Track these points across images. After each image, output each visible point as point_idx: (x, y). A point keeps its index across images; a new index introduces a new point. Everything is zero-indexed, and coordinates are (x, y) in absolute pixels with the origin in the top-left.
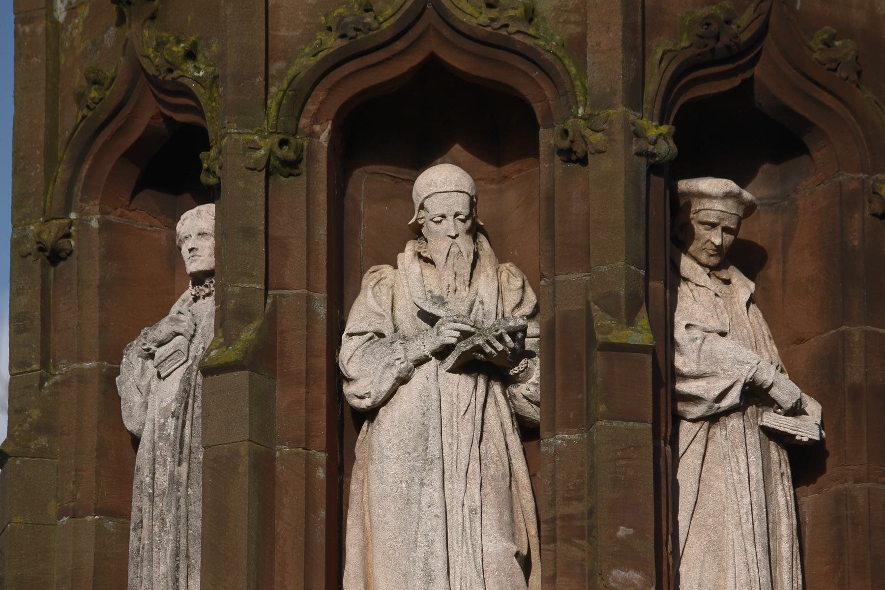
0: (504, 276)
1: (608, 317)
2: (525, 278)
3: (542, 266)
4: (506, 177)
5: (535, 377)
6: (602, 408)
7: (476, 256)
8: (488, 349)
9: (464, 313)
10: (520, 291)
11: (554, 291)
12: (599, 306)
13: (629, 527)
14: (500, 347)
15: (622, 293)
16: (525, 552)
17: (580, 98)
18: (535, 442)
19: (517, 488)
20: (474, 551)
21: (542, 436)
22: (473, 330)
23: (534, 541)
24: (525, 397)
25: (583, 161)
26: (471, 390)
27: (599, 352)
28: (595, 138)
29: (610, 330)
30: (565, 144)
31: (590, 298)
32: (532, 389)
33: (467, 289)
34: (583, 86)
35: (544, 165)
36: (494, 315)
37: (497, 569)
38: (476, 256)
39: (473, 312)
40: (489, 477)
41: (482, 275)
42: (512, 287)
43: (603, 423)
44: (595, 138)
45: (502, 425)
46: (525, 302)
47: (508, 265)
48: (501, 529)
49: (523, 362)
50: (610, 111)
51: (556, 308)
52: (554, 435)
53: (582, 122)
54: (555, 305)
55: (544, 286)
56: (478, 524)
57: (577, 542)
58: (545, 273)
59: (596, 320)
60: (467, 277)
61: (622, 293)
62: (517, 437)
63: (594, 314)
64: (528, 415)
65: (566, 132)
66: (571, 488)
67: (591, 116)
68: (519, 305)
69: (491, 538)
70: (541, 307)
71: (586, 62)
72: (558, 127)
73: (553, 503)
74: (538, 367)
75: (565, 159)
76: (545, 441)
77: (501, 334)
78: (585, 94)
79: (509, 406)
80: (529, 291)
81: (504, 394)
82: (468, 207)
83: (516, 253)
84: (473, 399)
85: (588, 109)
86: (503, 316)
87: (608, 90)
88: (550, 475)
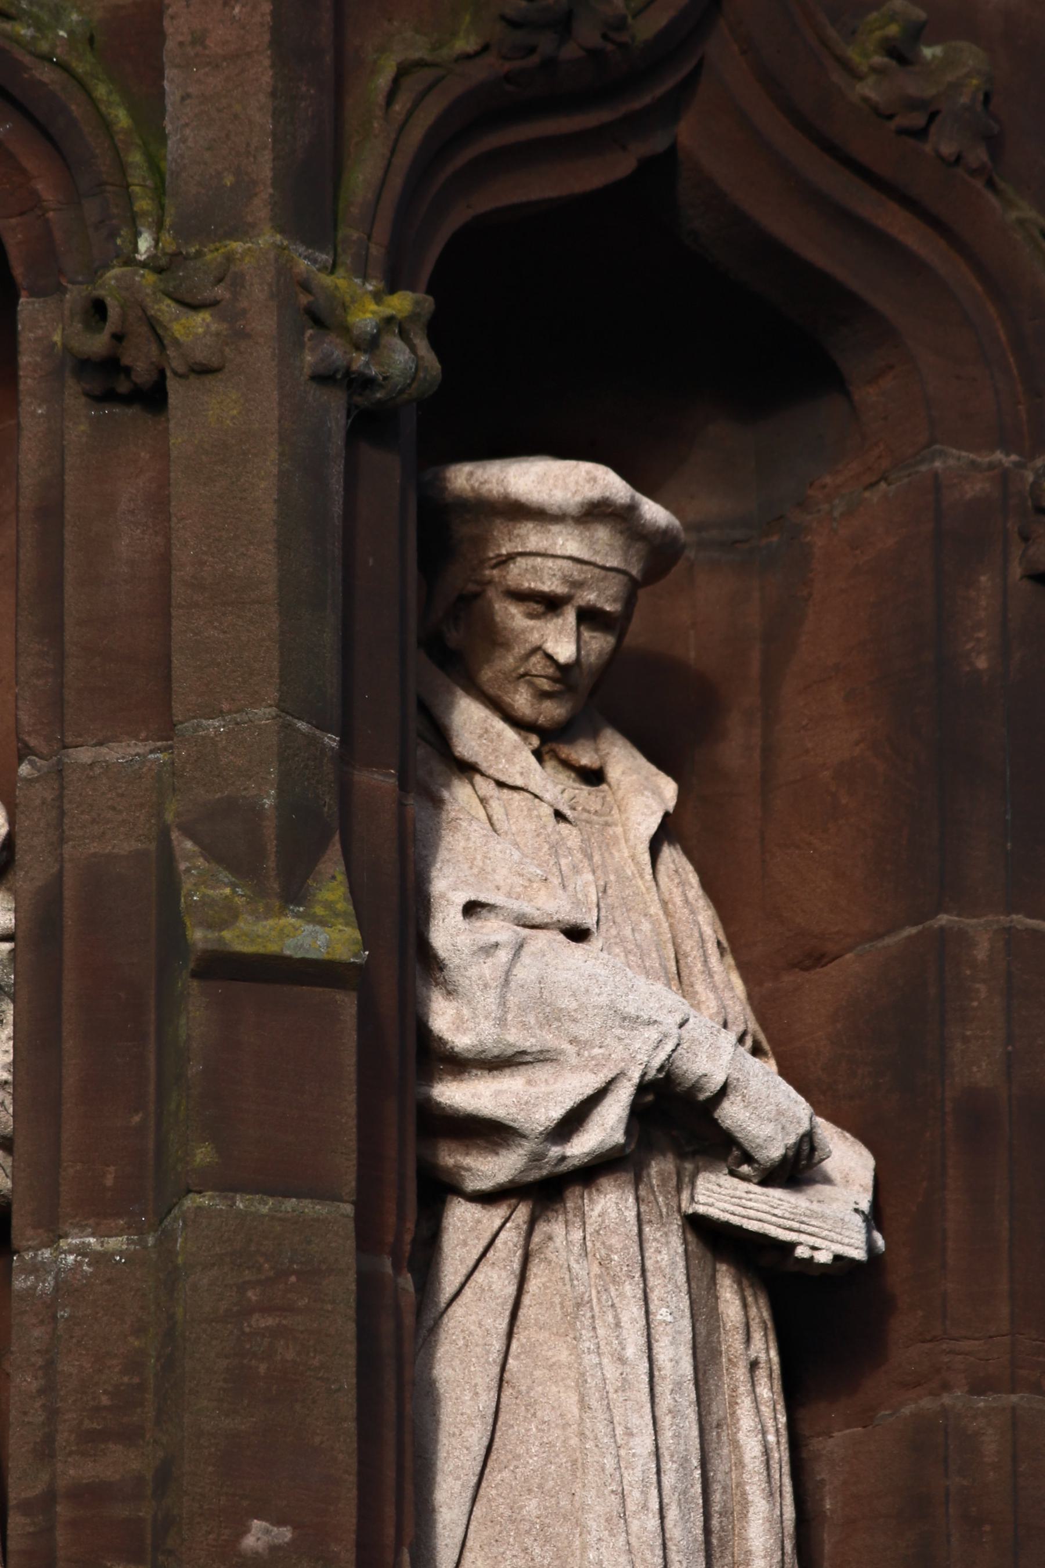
1: (225, 876)
3: (24, 718)
6: (203, 1155)
11: (60, 797)
12: (196, 841)
13: (279, 1523)
15: (268, 802)
17: (144, 204)
21: (17, 1241)
25: (153, 398)
27: (195, 983)
28: (193, 329)
29: (229, 915)
30: (97, 344)
31: (169, 817)
34: (154, 166)
35: (33, 411)
43: (204, 1200)
44: (193, 329)
50: (237, 246)
51: (67, 848)
52: (54, 1238)
53: (148, 279)
54: (62, 840)
55: (29, 781)
58: (33, 742)
59: (187, 885)
61: (268, 802)
63: (183, 866)
65: (98, 309)
66: (105, 1400)
67: (177, 259)
70: (20, 843)
71: (162, 94)
72: (75, 295)
73: (45, 1451)
76: (28, 1256)
78: (159, 192)
85: (166, 237)
87: (229, 180)
88: (40, 1361)
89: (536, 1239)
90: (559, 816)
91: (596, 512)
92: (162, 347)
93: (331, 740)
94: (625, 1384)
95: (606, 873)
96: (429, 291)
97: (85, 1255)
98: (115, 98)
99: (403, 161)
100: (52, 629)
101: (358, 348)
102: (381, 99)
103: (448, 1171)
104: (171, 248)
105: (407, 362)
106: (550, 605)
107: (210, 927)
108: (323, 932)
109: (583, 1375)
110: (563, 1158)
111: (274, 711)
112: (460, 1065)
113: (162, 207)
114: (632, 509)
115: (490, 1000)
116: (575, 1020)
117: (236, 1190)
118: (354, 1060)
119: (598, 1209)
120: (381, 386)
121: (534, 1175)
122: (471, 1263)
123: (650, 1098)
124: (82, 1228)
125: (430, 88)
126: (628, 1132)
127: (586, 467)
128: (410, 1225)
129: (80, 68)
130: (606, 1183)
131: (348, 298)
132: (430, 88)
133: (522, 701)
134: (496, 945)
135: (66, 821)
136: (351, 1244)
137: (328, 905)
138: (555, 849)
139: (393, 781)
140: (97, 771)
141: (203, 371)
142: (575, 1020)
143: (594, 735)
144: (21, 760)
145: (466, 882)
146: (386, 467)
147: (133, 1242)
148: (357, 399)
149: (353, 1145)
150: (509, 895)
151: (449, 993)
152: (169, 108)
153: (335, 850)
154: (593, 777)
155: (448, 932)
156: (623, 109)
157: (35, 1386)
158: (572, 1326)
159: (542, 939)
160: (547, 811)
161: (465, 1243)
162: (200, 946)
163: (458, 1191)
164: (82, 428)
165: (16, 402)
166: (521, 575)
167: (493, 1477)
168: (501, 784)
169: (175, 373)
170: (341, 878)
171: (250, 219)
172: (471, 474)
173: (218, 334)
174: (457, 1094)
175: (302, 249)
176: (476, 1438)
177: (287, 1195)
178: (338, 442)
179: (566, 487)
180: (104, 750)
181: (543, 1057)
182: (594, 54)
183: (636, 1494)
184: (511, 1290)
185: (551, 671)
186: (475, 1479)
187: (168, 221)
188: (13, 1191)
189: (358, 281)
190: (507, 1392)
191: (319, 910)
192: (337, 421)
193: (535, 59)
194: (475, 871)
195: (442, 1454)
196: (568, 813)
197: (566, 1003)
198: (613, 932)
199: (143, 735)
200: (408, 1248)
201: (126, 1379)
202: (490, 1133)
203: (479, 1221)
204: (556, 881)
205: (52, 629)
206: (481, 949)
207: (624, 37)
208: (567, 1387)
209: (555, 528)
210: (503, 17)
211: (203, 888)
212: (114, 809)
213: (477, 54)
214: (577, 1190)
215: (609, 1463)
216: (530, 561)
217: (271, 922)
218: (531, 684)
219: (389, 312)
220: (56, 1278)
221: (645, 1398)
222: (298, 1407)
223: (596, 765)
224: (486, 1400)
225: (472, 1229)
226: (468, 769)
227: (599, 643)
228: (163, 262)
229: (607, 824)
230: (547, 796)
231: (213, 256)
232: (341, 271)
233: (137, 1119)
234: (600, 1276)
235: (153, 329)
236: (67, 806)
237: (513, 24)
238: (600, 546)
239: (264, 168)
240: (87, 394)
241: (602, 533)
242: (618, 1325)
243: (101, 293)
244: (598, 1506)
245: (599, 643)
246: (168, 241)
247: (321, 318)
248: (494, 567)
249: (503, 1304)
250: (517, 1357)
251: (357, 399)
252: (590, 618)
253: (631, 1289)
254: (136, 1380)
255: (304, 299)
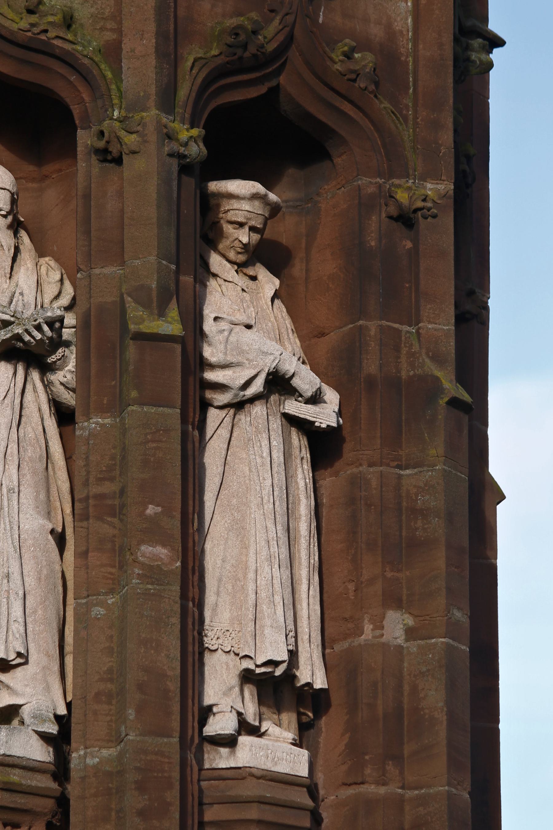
0: (43, 270)
1: (141, 308)
2: (63, 271)
3: (79, 259)
4: (47, 177)
5: (71, 365)
6: (134, 394)
7: (17, 250)
8: (27, 338)
9: (5, 304)
10: (59, 284)
11: (90, 284)
12: (132, 298)
13: (158, 506)
14: (39, 336)
15: (154, 286)
16: (60, 529)
17: (116, 101)
18: (71, 427)
19: (54, 469)
20: (11, 528)
21: (77, 420)
22: (12, 319)
23: (69, 519)
24: (62, 384)
25: (119, 161)
26: (11, 376)
27: (131, 341)
28: (130, 140)
30: (101, 144)
31: (123, 290)
32: (69, 376)
33: (8, 281)
34: (119, 90)
35: (81, 164)
36: (33, 306)
37: (33, 545)
38: (17, 250)
39: (14, 303)
40: (27, 459)
41: (22, 268)
42: (50, 280)
43: (134, 408)
44: (130, 140)
45: (40, 410)
46: (63, 294)
47: (47, 259)
48: (38, 507)
49: (60, 350)
51: (92, 299)
54: (90, 297)
55: (81, 279)
56: (15, 503)
57: (109, 519)
59: (129, 311)
60: (9, 270)
61: (154, 286)
62: (54, 421)
63: (127, 306)
64: (64, 401)
65: (102, 133)
67: (126, 118)
68: (57, 297)
69: (28, 516)
70: (78, 298)
72: (95, 129)
73: (86, 483)
74: (74, 356)
75: (101, 159)
77: (39, 324)
78: (121, 97)
79: (47, 392)
80: (67, 283)
81: (42, 381)
82: (9, 203)
83: (55, 248)
84: (12, 385)
86: (42, 307)
88: (84, 456)
89: (236, 420)
90: (243, 290)
91: (255, 197)
92: (121, 145)
93: (173, 267)
94: (263, 464)
95: (258, 308)
96: (203, 129)
97: (98, 424)
98: (107, 68)
99: (196, 88)
100: (88, 232)
101: (181, 146)
102: (189, 69)
103: (209, 399)
104: (124, 115)
105: (196, 150)
106: (241, 225)
107: (136, 324)
108: (171, 325)
109: (250, 461)
110: (244, 395)
111: (156, 258)
112: (212, 367)
113: (121, 102)
114: (266, 195)
115: (222, 347)
116: (248, 353)
117: (144, 405)
118: (180, 365)
119: (255, 411)
120: (189, 158)
121: (235, 401)
122: (216, 428)
123: (271, 377)
124: (97, 416)
125: (204, 66)
126: (264, 388)
127: (252, 183)
128: (197, 416)
129: (96, 59)
130: (257, 403)
131: (178, 130)
132: (204, 66)
133: (232, 255)
134: (224, 330)
135: (92, 291)
136: (179, 421)
137: (172, 318)
138: (242, 301)
139: (192, 279)
140: (101, 276)
141: (134, 152)
142: (248, 353)
143: (254, 265)
144: (78, 273)
145: (215, 311)
146: (190, 182)
147: (113, 421)
148: (181, 161)
149: (180, 391)
150: (228, 315)
151: (209, 345)
152: (124, 71)
153: (174, 300)
154: (254, 278)
155: (209, 326)
156: (263, 73)
157: (83, 464)
158: (247, 446)
159: (237, 329)
160: (239, 289)
161: (214, 421)
162: (133, 330)
163: (212, 406)
164: (97, 170)
165: (77, 162)
166: (231, 216)
167: (223, 492)
168: (225, 281)
169: (125, 153)
170: (176, 309)
171: (148, 106)
172: (216, 185)
173: (138, 141)
174: (211, 376)
175: (164, 115)
176: (217, 480)
177: (160, 406)
178: (175, 174)
179: (245, 189)
180: (103, 269)
181: (238, 365)
182: (254, 56)
183: (266, 498)
184: (228, 436)
185: (241, 246)
186: (217, 493)
187: (123, 107)
188: (76, 405)
189: (182, 125)
190: (227, 467)
191: (169, 319)
192: (175, 168)
193: (236, 57)
194: (217, 307)
195: (207, 485)
196: (246, 289)
197: (245, 348)
198: (260, 326)
199: (115, 265)
200: (196, 423)
201: (110, 462)
202: (221, 387)
203: (218, 415)
204: (242, 310)
205: (88, 232)
206: (219, 331)
207: (263, 50)
208: (245, 465)
209: (242, 202)
210: (226, 44)
211: (134, 313)
212: (106, 288)
213: (218, 55)
214: (249, 405)
215: (258, 488)
216: (235, 211)
217: (155, 323)
218: (234, 249)
219: (191, 135)
220: (89, 431)
221: (269, 468)
222: (163, 471)
223: (254, 275)
224: (221, 469)
225: (216, 417)
226: (215, 276)
227: (256, 237)
228: (122, 119)
229: (258, 293)
230: (240, 284)
231: (137, 117)
232: (176, 122)
233: (113, 383)
234: (255, 431)
235: (119, 139)
236: (92, 287)
237: (229, 46)
238: (257, 207)
239: (153, 90)
240: (98, 160)
241: (257, 203)
242: (261, 446)
243: (103, 128)
244: (254, 501)
245: (256, 237)
246: (123, 113)
247: (170, 137)
248: (223, 213)
249: (226, 440)
250: (230, 456)
251: (181, 161)
252: (252, 229)
253: (265, 436)
254: (114, 462)
255: (165, 131)
